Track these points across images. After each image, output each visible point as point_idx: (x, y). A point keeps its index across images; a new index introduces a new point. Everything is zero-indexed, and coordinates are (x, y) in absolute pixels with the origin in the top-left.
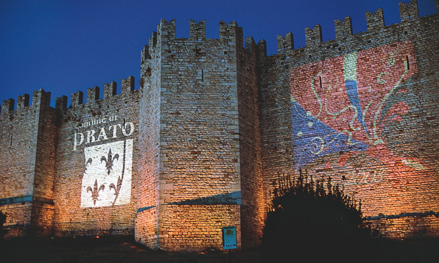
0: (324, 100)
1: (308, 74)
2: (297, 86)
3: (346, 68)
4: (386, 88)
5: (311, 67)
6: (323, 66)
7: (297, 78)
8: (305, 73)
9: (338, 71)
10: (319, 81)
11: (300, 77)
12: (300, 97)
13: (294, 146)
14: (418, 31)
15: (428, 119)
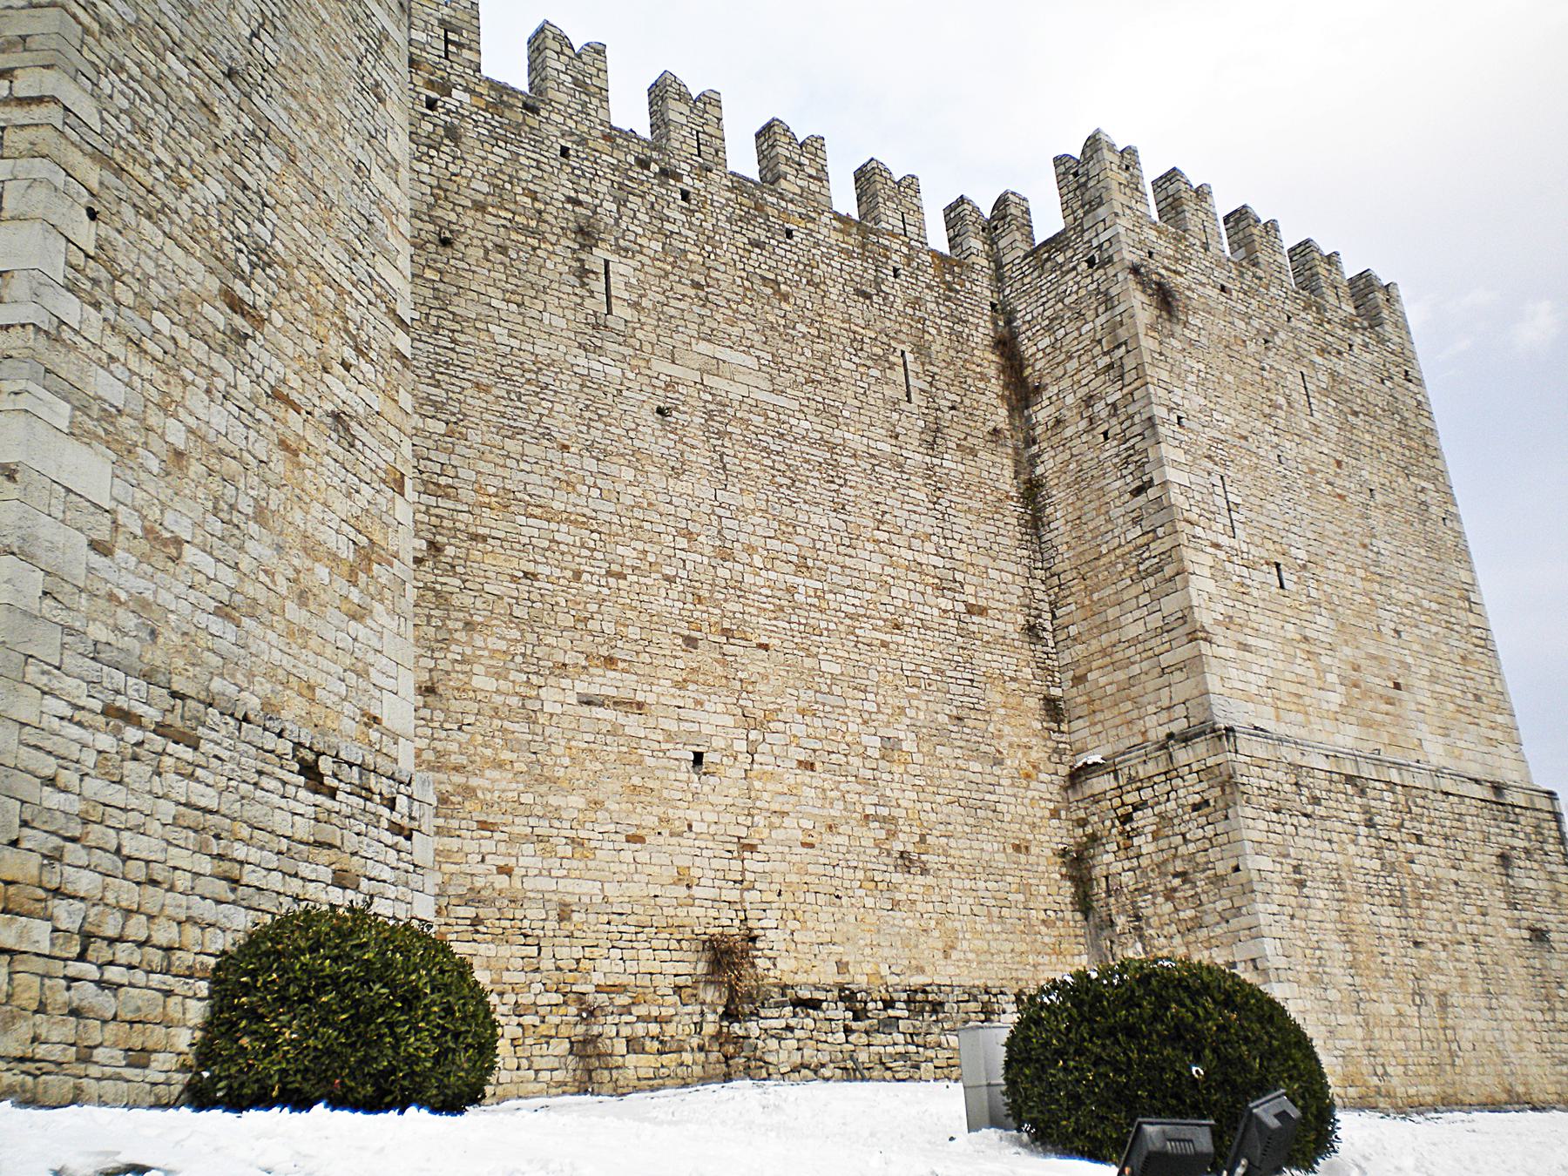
0: (619, 373)
1: (553, 221)
2: (502, 249)
3: (708, 286)
4: (847, 435)
5: (569, 199)
6: (617, 224)
7: (503, 213)
8: (540, 212)
9: (680, 282)
10: (603, 278)
11: (517, 218)
12: (513, 307)
13: (474, 537)
14: (929, 287)
15: (971, 610)
